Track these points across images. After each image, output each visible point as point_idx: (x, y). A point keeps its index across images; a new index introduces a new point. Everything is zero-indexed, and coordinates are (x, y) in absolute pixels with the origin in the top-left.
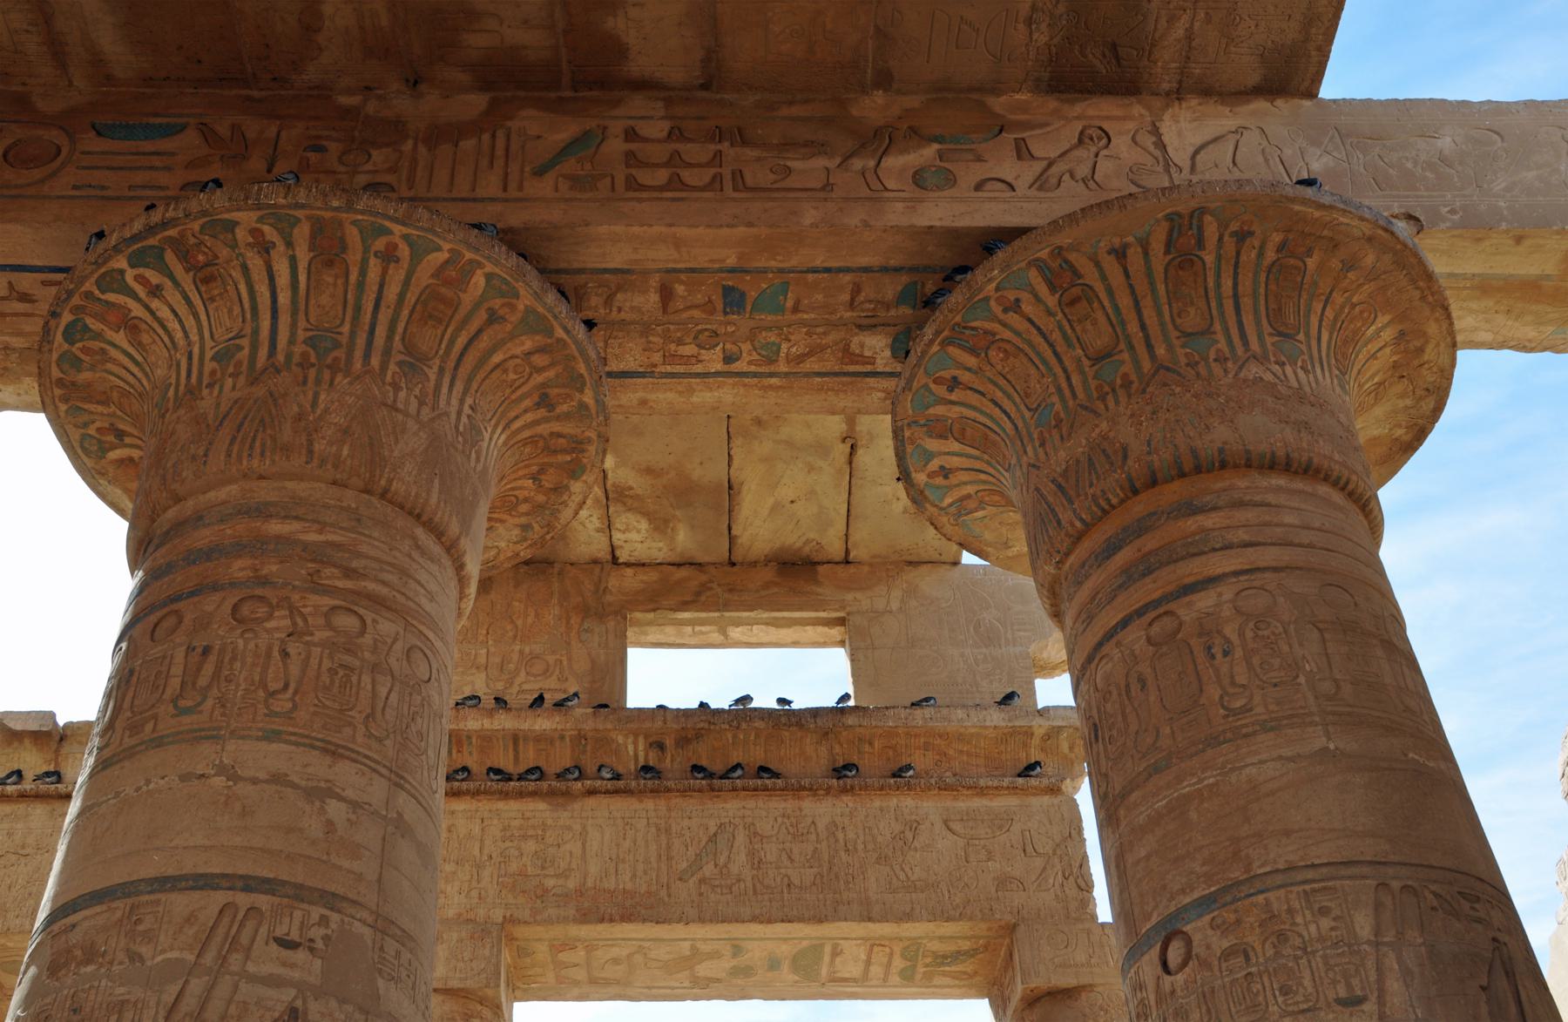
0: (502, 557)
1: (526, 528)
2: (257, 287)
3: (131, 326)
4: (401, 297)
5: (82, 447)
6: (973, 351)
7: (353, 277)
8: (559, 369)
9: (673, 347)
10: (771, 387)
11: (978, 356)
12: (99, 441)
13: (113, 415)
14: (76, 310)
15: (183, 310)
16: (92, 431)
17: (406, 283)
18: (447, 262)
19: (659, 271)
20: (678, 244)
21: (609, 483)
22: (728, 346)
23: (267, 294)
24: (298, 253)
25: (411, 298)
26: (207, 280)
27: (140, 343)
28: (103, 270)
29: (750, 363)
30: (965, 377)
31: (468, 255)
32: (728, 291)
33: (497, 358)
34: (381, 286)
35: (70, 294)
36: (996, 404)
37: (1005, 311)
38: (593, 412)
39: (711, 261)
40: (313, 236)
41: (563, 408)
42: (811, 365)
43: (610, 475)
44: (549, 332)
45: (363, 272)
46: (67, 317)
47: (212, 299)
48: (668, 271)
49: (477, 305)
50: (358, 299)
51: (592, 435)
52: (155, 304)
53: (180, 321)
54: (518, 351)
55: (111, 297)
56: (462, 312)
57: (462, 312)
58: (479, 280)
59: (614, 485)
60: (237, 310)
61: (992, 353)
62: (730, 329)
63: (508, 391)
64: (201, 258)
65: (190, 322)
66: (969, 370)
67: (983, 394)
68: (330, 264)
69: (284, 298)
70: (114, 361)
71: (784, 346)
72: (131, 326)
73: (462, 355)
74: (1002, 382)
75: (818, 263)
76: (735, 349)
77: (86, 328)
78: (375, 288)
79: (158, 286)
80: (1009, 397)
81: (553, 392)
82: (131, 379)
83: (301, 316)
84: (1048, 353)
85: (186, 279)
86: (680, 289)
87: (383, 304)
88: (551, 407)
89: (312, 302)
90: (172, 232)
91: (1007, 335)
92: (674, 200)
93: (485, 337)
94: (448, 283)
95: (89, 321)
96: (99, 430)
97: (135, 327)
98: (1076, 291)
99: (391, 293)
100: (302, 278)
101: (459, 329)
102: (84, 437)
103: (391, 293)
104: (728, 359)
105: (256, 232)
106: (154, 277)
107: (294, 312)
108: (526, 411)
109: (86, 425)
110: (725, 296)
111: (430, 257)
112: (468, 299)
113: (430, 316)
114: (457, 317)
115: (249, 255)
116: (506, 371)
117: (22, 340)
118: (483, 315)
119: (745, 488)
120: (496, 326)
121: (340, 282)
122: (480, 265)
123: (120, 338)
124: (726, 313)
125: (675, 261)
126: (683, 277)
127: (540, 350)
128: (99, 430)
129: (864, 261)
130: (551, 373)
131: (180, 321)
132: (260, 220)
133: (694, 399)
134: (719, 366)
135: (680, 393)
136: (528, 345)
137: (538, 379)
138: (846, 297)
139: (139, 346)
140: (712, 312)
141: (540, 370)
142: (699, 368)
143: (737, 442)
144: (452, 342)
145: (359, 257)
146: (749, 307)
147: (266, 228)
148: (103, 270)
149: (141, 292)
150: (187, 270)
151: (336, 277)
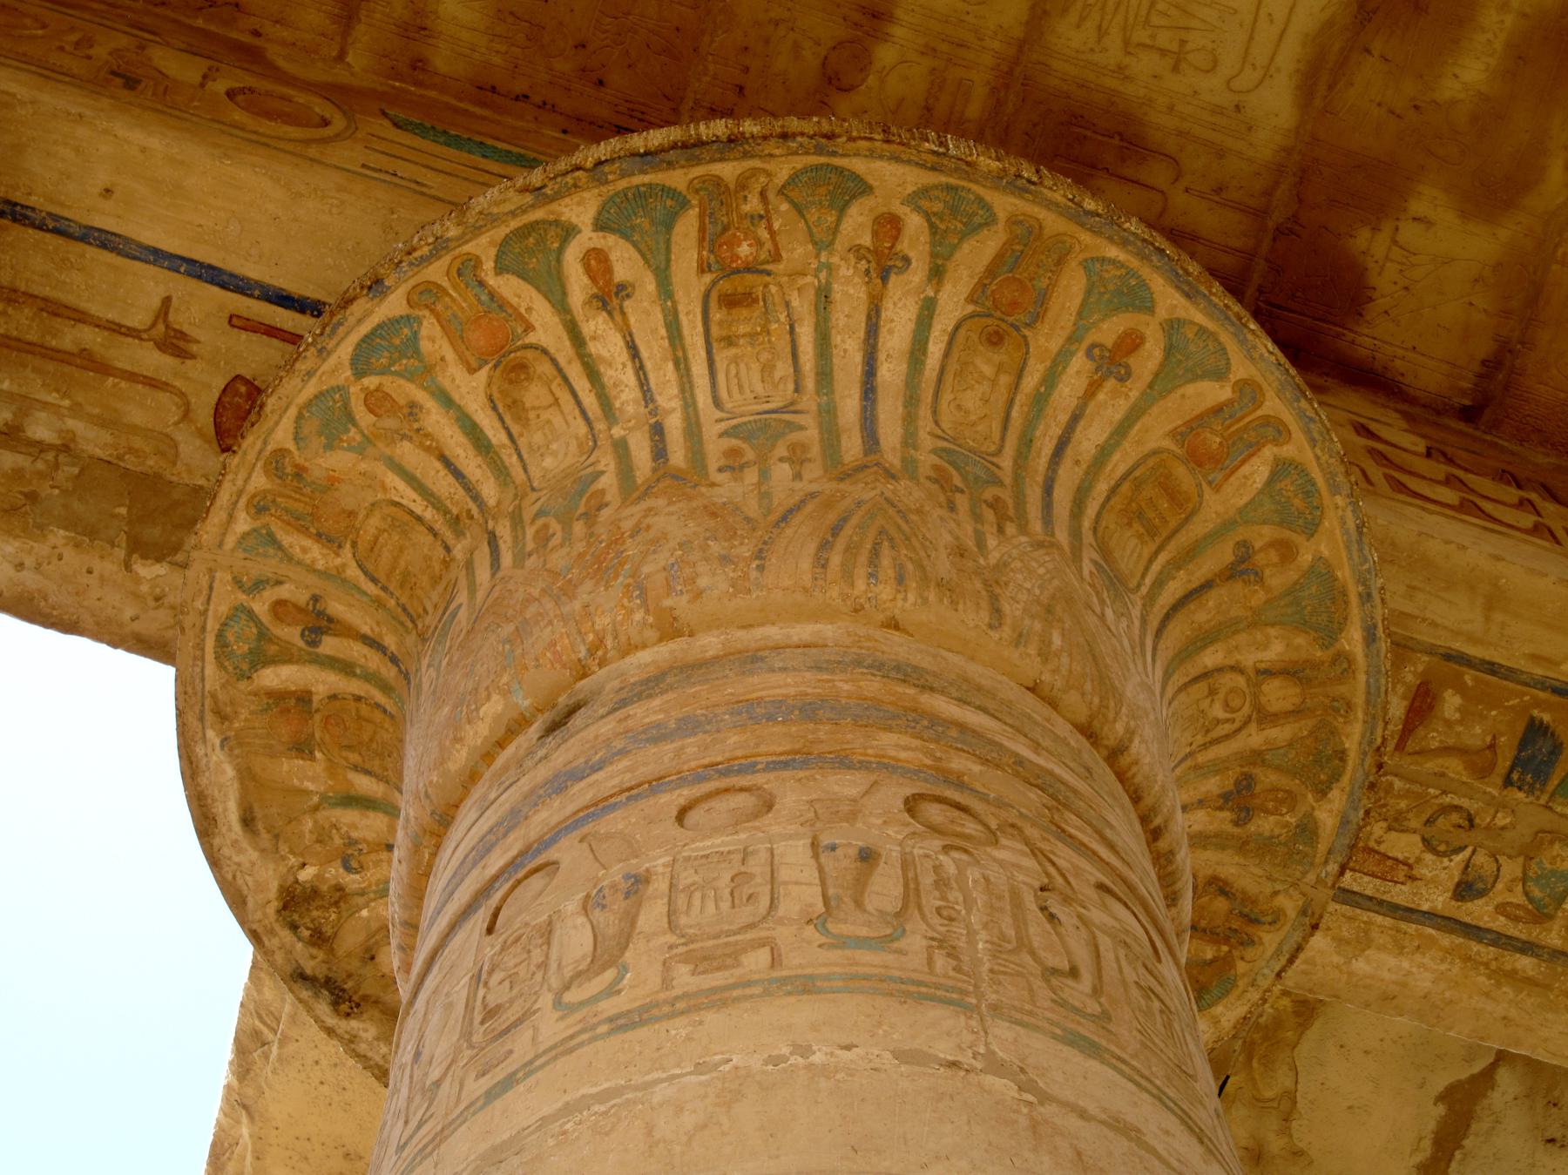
2: (837, 339)
3: (511, 364)
4: (1104, 453)
5: (220, 636)
7: (1030, 382)
8: (1304, 727)
9: (1378, 829)
10: (1512, 975)
12: (263, 635)
13: (335, 576)
14: (427, 295)
15: (653, 349)
16: (261, 607)
17: (1121, 431)
18: (1217, 410)
19: (1431, 650)
20: (1494, 599)
22: (1481, 858)
23: (858, 358)
24: (943, 297)
25: (1119, 463)
26: (731, 302)
27: (515, 405)
28: (539, 214)
29: (1501, 909)
31: (1273, 405)
32: (1535, 731)
33: (1211, 658)
34: (1075, 418)
35: (441, 246)
38: (1322, 848)
39: (1536, 658)
40: (991, 271)
41: (1264, 825)
44: (1330, 633)
45: (1051, 379)
46: (394, 305)
47: (730, 341)
48: (1449, 657)
49: (1227, 526)
50: (1030, 424)
51: (1289, 905)
52: (596, 325)
53: (640, 370)
54: (1249, 659)
55: (509, 287)
56: (1199, 528)
57: (1199, 528)
58: (1258, 471)
60: (783, 369)
62: (1502, 820)
63: (1200, 739)
65: (664, 377)
68: (995, 339)
69: (890, 372)
70: (423, 438)
72: (511, 364)
73: (1167, 617)
77: (411, 347)
78: (1064, 418)
79: (621, 287)
81: (1267, 778)
82: (443, 484)
83: (924, 412)
85: (690, 285)
86: (1451, 703)
87: (1069, 452)
88: (1244, 814)
89: (947, 396)
90: (728, 170)
92: (1485, 528)
93: (1212, 599)
94: (1197, 459)
95: (429, 328)
96: (279, 607)
97: (522, 367)
99: (1089, 438)
100: (935, 349)
101: (1177, 564)
103: (1089, 438)
104: (1465, 889)
105: (889, 225)
106: (625, 262)
107: (911, 400)
108: (1201, 803)
109: (258, 586)
110: (1523, 744)
111: (1190, 389)
112: (1217, 505)
113: (1140, 515)
114: (1183, 539)
115: (845, 271)
116: (1212, 692)
117: (106, 437)
118: (1222, 555)
120: (1238, 587)
121: (1005, 379)
122: (1280, 432)
123: (471, 388)
124: (1508, 782)
125: (1471, 639)
126: (1469, 677)
127: (1290, 672)
128: (279, 607)
130: (1280, 734)
131: (640, 370)
132: (916, 199)
133: (1360, 966)
134: (1438, 900)
135: (1340, 941)
136: (1275, 649)
137: (1254, 738)
139: (508, 406)
140: (1483, 772)
141: (1265, 717)
142: (1400, 894)
144: (1159, 584)
145: (1055, 345)
146: (1554, 782)
147: (914, 222)
148: (539, 214)
149: (578, 287)
150: (703, 268)
151: (1000, 368)
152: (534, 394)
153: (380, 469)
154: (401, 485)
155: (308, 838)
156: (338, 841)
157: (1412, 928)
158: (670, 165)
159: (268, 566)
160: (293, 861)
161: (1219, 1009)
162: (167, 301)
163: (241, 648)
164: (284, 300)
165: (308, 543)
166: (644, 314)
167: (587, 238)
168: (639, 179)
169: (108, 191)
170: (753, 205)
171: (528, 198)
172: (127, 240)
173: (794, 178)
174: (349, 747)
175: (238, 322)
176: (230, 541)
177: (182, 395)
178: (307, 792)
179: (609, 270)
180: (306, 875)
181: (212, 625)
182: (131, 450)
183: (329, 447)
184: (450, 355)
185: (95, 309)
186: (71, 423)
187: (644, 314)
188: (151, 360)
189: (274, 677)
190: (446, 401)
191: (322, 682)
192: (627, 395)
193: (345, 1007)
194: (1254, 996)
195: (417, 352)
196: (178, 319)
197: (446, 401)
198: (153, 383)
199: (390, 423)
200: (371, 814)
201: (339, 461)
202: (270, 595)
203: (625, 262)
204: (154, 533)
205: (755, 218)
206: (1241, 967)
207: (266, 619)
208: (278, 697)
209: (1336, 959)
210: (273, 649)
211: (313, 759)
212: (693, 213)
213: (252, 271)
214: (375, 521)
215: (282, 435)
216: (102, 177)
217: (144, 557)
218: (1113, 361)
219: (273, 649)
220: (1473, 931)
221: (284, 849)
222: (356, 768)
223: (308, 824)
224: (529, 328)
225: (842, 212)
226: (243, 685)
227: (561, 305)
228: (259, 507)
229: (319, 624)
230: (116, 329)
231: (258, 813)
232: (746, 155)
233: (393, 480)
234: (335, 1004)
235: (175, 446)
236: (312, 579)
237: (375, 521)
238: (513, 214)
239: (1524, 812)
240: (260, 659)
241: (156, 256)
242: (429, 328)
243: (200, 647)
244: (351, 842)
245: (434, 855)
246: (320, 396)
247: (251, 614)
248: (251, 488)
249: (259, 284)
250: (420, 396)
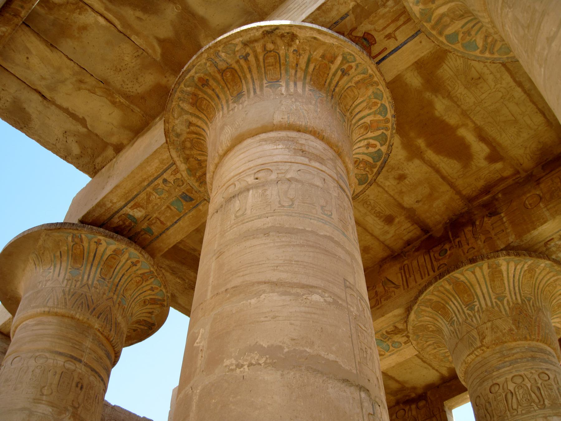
0: (171, 117)
1: (178, 135)
3: (367, 128)
5: (353, 55)
6: (143, 274)
10: (144, 180)
11: (141, 274)
12: (348, 62)
13: (350, 81)
14: (387, 121)
21: (90, 10)
22: (171, 185)
28: (387, 143)
30: (135, 268)
32: (191, 199)
36: (123, 275)
37: (152, 287)
42: (143, 195)
43: (94, 14)
55: (379, 132)
59: (86, 10)
61: (139, 278)
62: (177, 190)
64: (362, 165)
66: (137, 270)
67: (127, 271)
70: (365, 108)
71: (157, 196)
74: (129, 279)
75: (180, 222)
76: (168, 185)
77: (380, 113)
79: (368, 148)
80: (125, 281)
82: (357, 110)
84: (135, 296)
90: (375, 170)
91: (144, 284)
95: (381, 118)
96: (351, 67)
98: (147, 303)
102: (355, 61)
104: (165, 181)
106: (371, 150)
109: (357, 66)
117: (381, 14)
119: (49, 51)
123: (368, 120)
128: (351, 67)
129: (171, 231)
134: (165, 176)
135: (164, 160)
138: (162, 219)
142: (169, 172)
143: (77, 68)
148: (387, 143)
149: (372, 142)
153: (364, 98)
154: (360, 101)
155: (305, 47)
156: (301, 52)
157: (161, 171)
158: (382, 164)
159: (360, 69)
160: (302, 41)
161: (186, 172)
162: (397, 40)
163: (348, 57)
164: (383, 59)
165: (359, 79)
166: (364, 150)
167: (379, 146)
168: (383, 159)
169: (421, 42)
170: (367, 169)
171: (391, 144)
172: (411, 40)
173: (368, 177)
174: (319, 67)
175: (385, 49)
176: (369, 68)
177: (379, 32)
178: (314, 52)
179: (372, 147)
180: (297, 41)
181: (356, 55)
182: (376, 16)
183: (373, 92)
184: (375, 119)
185: (404, 27)
186: (388, 9)
188: (389, 30)
189: (339, 59)
190: (368, 115)
191: (334, 67)
193: (265, 32)
194: (186, 179)
195: (378, 114)
196: (392, 40)
197: (368, 115)
198: (385, 28)
199: (371, 104)
200: (305, 65)
201: (370, 92)
202: (354, 67)
203: (371, 150)
204: (358, 10)
205: (365, 169)
206: (193, 178)
207: (350, 64)
208: (335, 58)
209: (160, 158)
210: (344, 62)
211: (320, 57)
212: (372, 162)
213: (392, 57)
214: (356, 93)
215: (380, 87)
216: (423, 43)
217: (355, 6)
219: (344, 62)
220: (156, 179)
221: (305, 41)
222: (315, 66)
223: (308, 48)
224: (371, 132)
225: (358, 180)
226: (341, 53)
227: (371, 138)
228: (371, 76)
229: (344, 73)
230: (398, 28)
231: (315, 41)
232: (376, 174)
233: (362, 99)
234: (267, 31)
235: (371, 24)
236: (352, 76)
237: (356, 93)
238: (390, 140)
239: (177, 192)
240: (344, 58)
241: (405, 43)
242: (381, 118)
243: (354, 52)
244: (300, 55)
245: (334, 150)
246: (383, 97)
247: (353, 62)
248: (375, 77)
249: (389, 56)
250: (372, 111)
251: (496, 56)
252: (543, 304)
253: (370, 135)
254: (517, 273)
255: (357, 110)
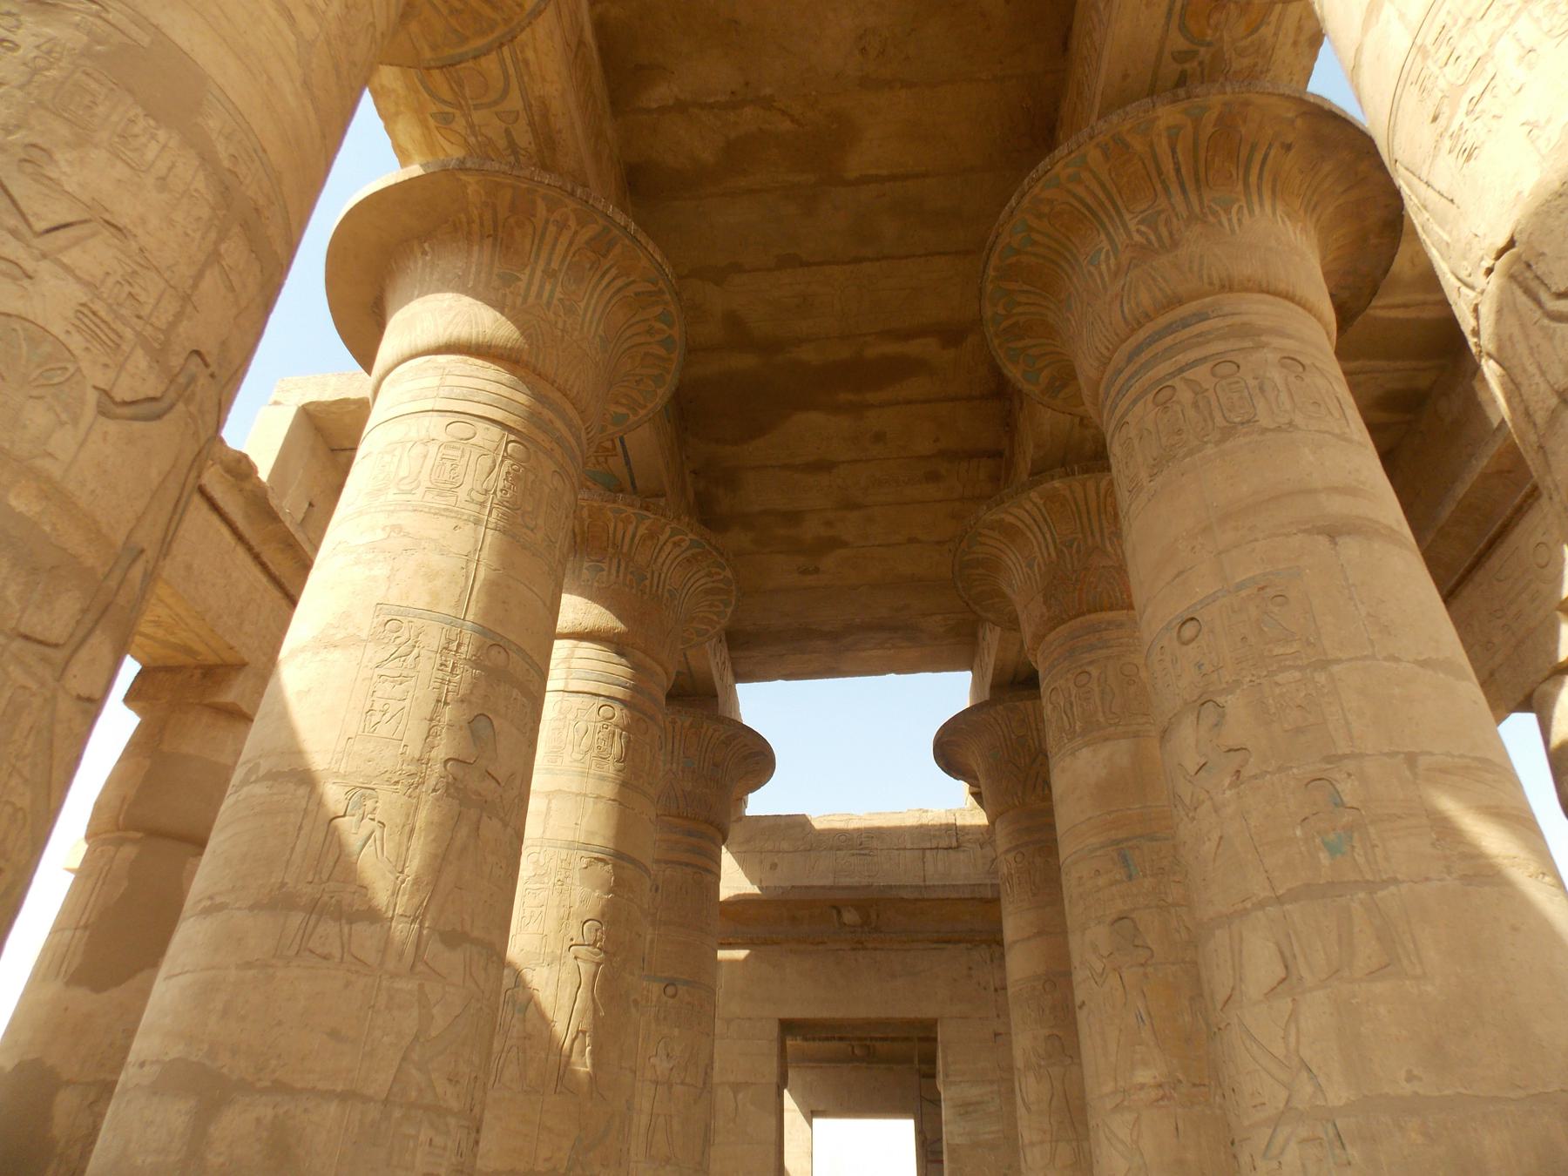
52: (669, 546)
82: (619, 535)
85: (689, 553)
123: (642, 531)
152: (649, 543)
166: (677, 551)
187: (677, 551)
192: (660, 560)
218: (711, 606)
251: (650, 406)
252: (1106, 532)
253: (663, 538)
254: (1035, 512)
255: (619, 535)
